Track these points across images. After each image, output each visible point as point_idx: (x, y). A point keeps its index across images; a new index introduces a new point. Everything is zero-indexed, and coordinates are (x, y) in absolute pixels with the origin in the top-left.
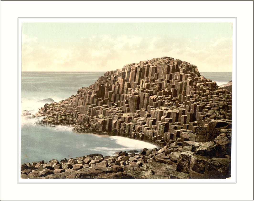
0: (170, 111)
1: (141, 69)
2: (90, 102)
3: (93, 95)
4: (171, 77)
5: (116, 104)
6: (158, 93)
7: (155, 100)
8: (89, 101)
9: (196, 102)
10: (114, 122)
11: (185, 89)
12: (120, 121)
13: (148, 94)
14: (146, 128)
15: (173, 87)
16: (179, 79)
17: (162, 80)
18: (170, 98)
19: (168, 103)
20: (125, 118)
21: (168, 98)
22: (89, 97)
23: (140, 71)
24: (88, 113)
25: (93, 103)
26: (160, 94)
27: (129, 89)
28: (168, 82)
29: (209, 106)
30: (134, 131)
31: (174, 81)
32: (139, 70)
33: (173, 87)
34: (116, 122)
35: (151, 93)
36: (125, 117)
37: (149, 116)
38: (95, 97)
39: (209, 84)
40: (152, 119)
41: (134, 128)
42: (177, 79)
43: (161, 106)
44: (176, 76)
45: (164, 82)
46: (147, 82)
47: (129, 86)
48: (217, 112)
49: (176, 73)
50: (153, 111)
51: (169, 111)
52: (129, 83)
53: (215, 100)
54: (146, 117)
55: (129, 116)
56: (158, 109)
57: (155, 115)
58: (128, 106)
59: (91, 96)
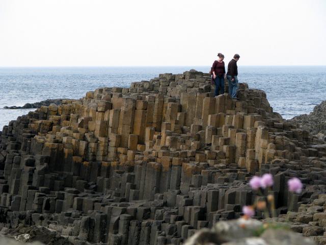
0: (235, 191)
1: (145, 103)
2: (34, 184)
3: (39, 168)
4: (219, 123)
5: (94, 186)
6: (198, 156)
7: (196, 171)
8: (30, 182)
9: (282, 171)
10: (114, 219)
11: (253, 146)
12: (128, 217)
13: (180, 160)
14: (186, 227)
15: (227, 142)
16: (238, 126)
17: (201, 128)
18: (224, 166)
19: (223, 176)
20: (136, 211)
21: (221, 165)
22: (32, 172)
23: (145, 109)
24: (36, 207)
25: (43, 186)
26: (204, 158)
27: (121, 150)
28: (215, 131)
29: (305, 178)
30: (162, 235)
31: (226, 131)
32: (140, 105)
33: (227, 142)
34: (119, 219)
35: (185, 158)
36: (136, 208)
37: (189, 203)
38: (46, 171)
39: (299, 134)
40: (197, 208)
41: (160, 228)
42: (233, 125)
43: (209, 183)
44: (231, 120)
45: (205, 133)
46: (170, 134)
47: (120, 142)
48: (322, 187)
49: (228, 112)
50: (196, 193)
51: (231, 190)
52: (119, 136)
53: (314, 167)
54: (184, 206)
55: (142, 206)
56: (205, 189)
57: (204, 200)
58: (134, 187)
59: (35, 169)
